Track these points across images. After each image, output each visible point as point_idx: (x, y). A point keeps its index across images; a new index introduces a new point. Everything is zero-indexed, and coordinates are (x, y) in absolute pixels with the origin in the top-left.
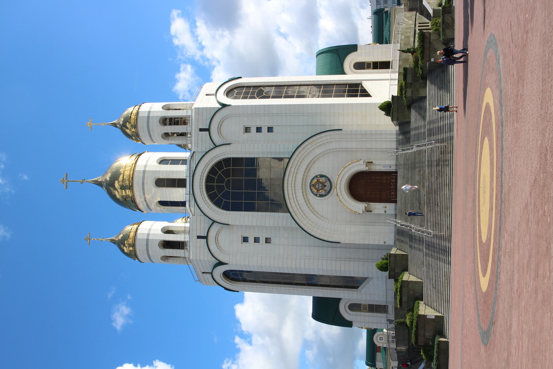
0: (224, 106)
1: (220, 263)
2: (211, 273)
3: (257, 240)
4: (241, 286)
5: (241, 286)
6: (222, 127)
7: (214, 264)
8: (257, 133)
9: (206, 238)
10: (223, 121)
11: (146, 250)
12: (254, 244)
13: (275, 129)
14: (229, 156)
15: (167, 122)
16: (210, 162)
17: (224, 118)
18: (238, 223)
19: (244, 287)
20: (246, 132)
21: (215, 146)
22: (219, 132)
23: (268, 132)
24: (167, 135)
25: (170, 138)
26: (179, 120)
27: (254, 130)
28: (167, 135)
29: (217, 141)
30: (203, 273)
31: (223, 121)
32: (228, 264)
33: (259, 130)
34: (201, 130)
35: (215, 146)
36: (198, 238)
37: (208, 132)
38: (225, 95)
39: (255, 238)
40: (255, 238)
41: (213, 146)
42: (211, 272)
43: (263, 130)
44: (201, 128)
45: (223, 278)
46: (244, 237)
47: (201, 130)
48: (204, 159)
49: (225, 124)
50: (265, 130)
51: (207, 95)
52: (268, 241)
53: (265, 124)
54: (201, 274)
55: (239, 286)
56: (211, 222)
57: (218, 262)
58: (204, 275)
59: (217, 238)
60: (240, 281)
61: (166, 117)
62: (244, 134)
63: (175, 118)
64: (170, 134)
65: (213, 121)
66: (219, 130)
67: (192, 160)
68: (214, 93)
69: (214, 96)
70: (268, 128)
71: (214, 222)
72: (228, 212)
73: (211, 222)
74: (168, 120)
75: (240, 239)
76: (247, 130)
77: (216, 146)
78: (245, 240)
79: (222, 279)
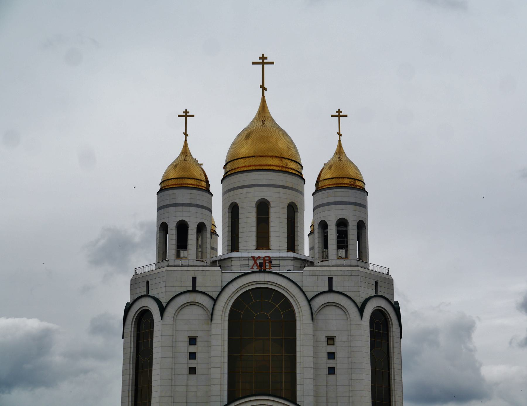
0: (361, 310)
1: (162, 310)
2: (147, 296)
3: (193, 356)
4: (131, 332)
5: (131, 332)
6: (334, 308)
7: (159, 299)
8: (327, 353)
9: (194, 290)
10: (341, 309)
11: (174, 203)
12: (188, 352)
13: (331, 377)
14: (298, 318)
15: (342, 227)
16: (289, 293)
17: (345, 310)
18: (213, 332)
19: (130, 336)
20: (328, 338)
21: (309, 298)
22: (327, 304)
23: (328, 368)
24: (323, 225)
25: (320, 231)
26: (345, 244)
27: (331, 349)
28: (323, 225)
29: (318, 303)
30: (148, 283)
31: (341, 309)
32: (162, 319)
33: (331, 356)
34: (330, 280)
35: (309, 298)
36: (193, 278)
37: (327, 289)
38: (377, 308)
39: (195, 353)
40: (195, 353)
41: (310, 295)
42: (150, 294)
43: (331, 361)
44: (333, 279)
45: (142, 309)
46: (196, 339)
47: (330, 280)
48: (294, 287)
49: (338, 311)
50: (331, 363)
51: (376, 283)
52: (192, 371)
53: (339, 363)
54: (147, 279)
55: (131, 330)
56: (214, 295)
57: (164, 305)
58: (145, 284)
59: (194, 304)
60: (137, 332)
61: (348, 227)
62: (326, 336)
63: (347, 238)
64: (326, 231)
65: (341, 297)
66: (330, 304)
67: (292, 258)
68: (380, 293)
69: (374, 294)
70: (334, 368)
71: (215, 301)
72: (227, 318)
73: (215, 298)
74: (344, 229)
75: (193, 334)
76: (331, 340)
77: (309, 301)
78: (193, 340)
79: (140, 308)
